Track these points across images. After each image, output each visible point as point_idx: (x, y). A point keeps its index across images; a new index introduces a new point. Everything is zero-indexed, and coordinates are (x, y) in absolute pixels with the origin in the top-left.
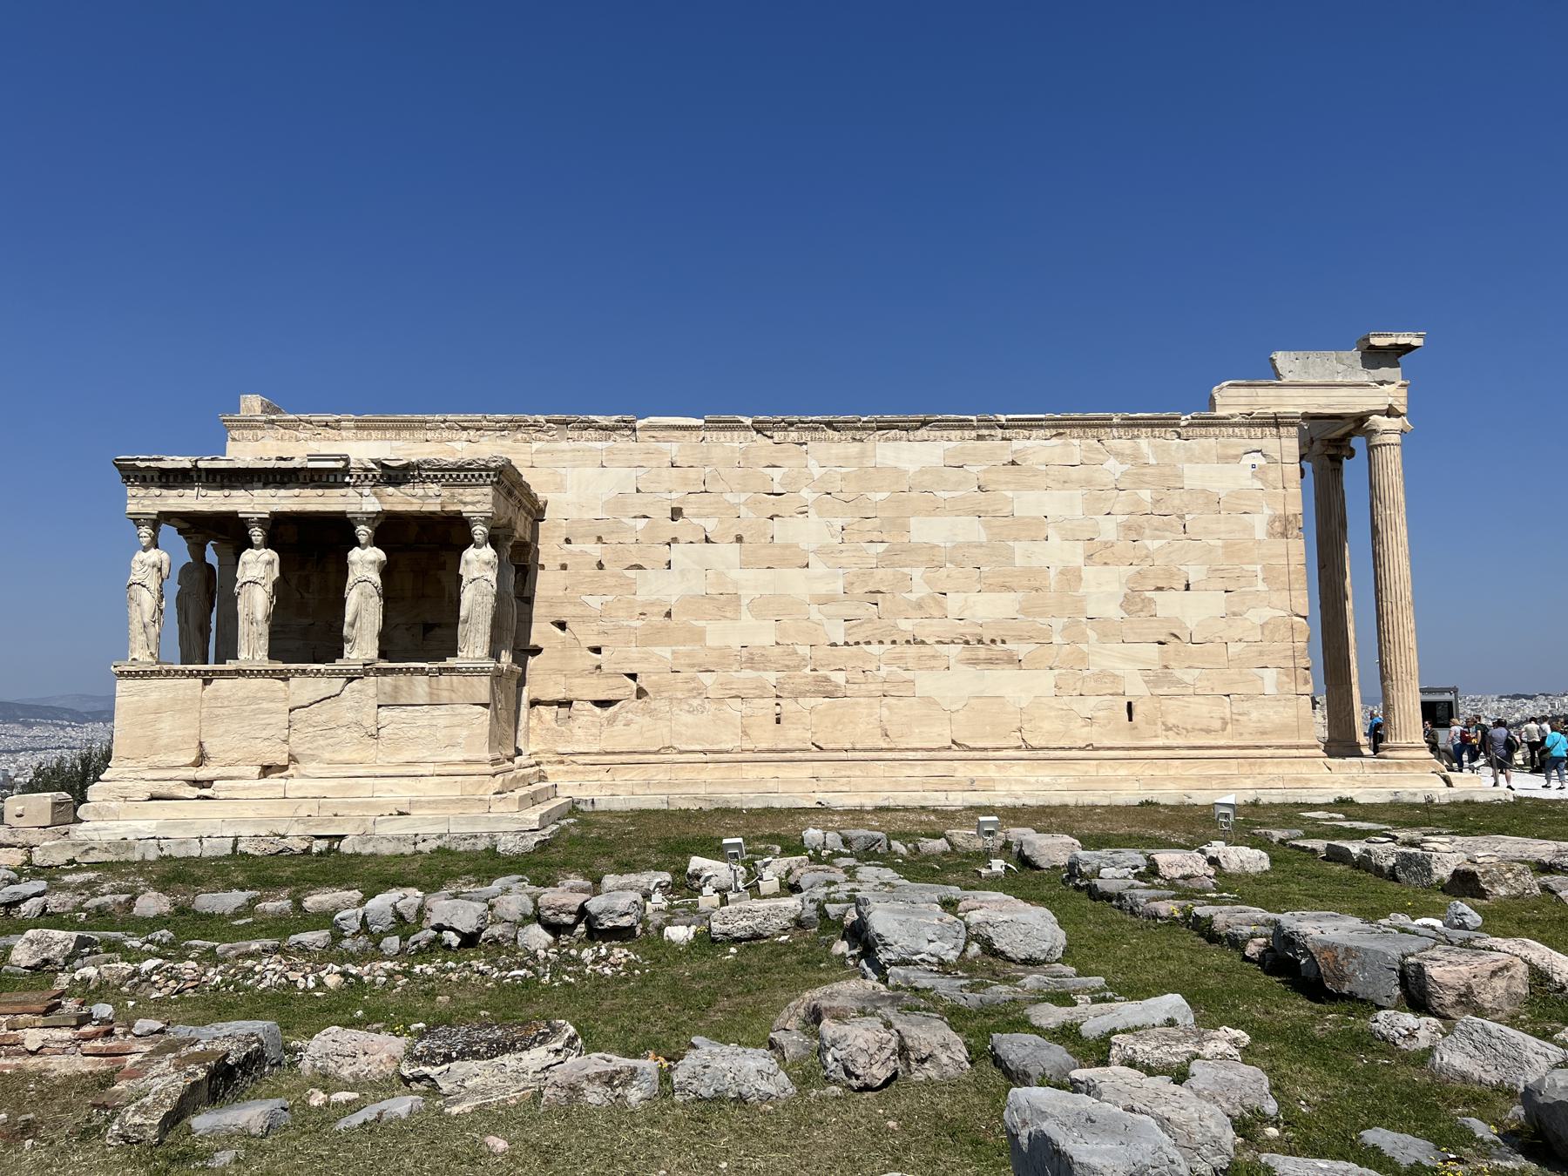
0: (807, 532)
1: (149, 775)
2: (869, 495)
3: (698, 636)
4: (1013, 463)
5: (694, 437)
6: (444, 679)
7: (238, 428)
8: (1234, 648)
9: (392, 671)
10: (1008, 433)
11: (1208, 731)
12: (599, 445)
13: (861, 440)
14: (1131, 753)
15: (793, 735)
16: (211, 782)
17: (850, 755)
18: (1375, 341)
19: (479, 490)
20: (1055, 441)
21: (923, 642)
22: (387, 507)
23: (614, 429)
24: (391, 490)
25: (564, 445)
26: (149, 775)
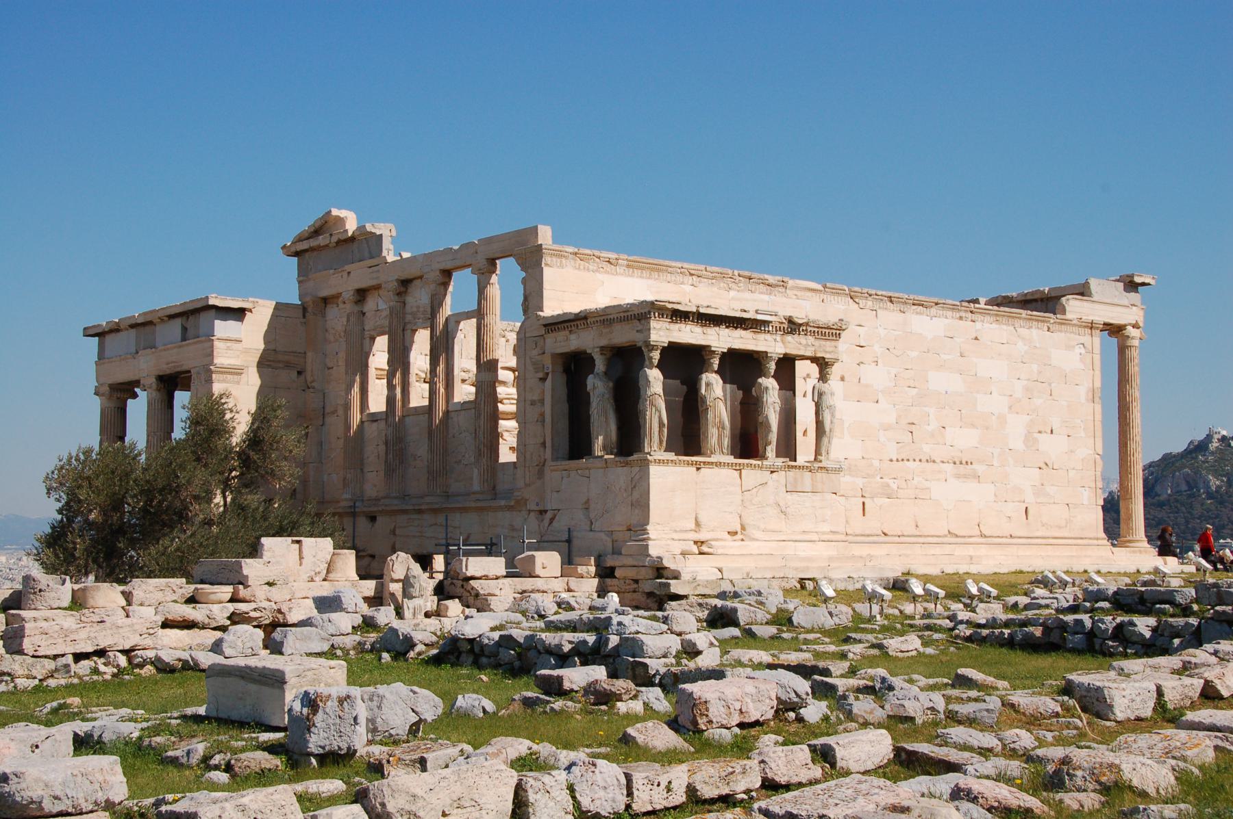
1: (676, 536)
4: (976, 339)
5: (816, 298)
6: (819, 475)
8: (1072, 473)
10: (974, 317)
11: (1060, 527)
12: (766, 297)
14: (1030, 540)
15: (872, 524)
17: (902, 539)
18: (1138, 280)
19: (833, 343)
20: (994, 326)
22: (788, 351)
25: (747, 295)
26: (676, 536)
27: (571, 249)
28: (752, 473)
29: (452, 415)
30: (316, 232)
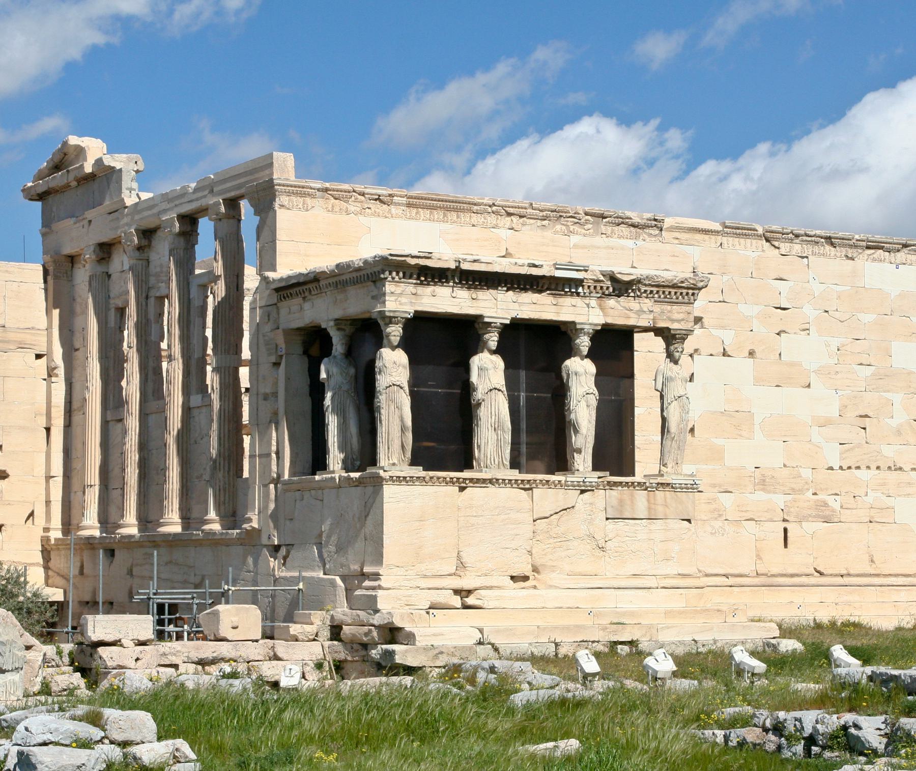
0: (808, 350)
1: (424, 583)
2: (861, 316)
3: (717, 455)
6: (660, 494)
7: (289, 194)
9: (620, 484)
12: (630, 243)
13: (852, 259)
15: (797, 559)
16: (469, 592)
17: (846, 580)
19: (684, 308)
21: (900, 469)
23: (643, 227)
24: (612, 302)
25: (599, 240)
26: (424, 583)
27: (318, 184)
28: (550, 494)
29: (195, 412)
30: (57, 167)
